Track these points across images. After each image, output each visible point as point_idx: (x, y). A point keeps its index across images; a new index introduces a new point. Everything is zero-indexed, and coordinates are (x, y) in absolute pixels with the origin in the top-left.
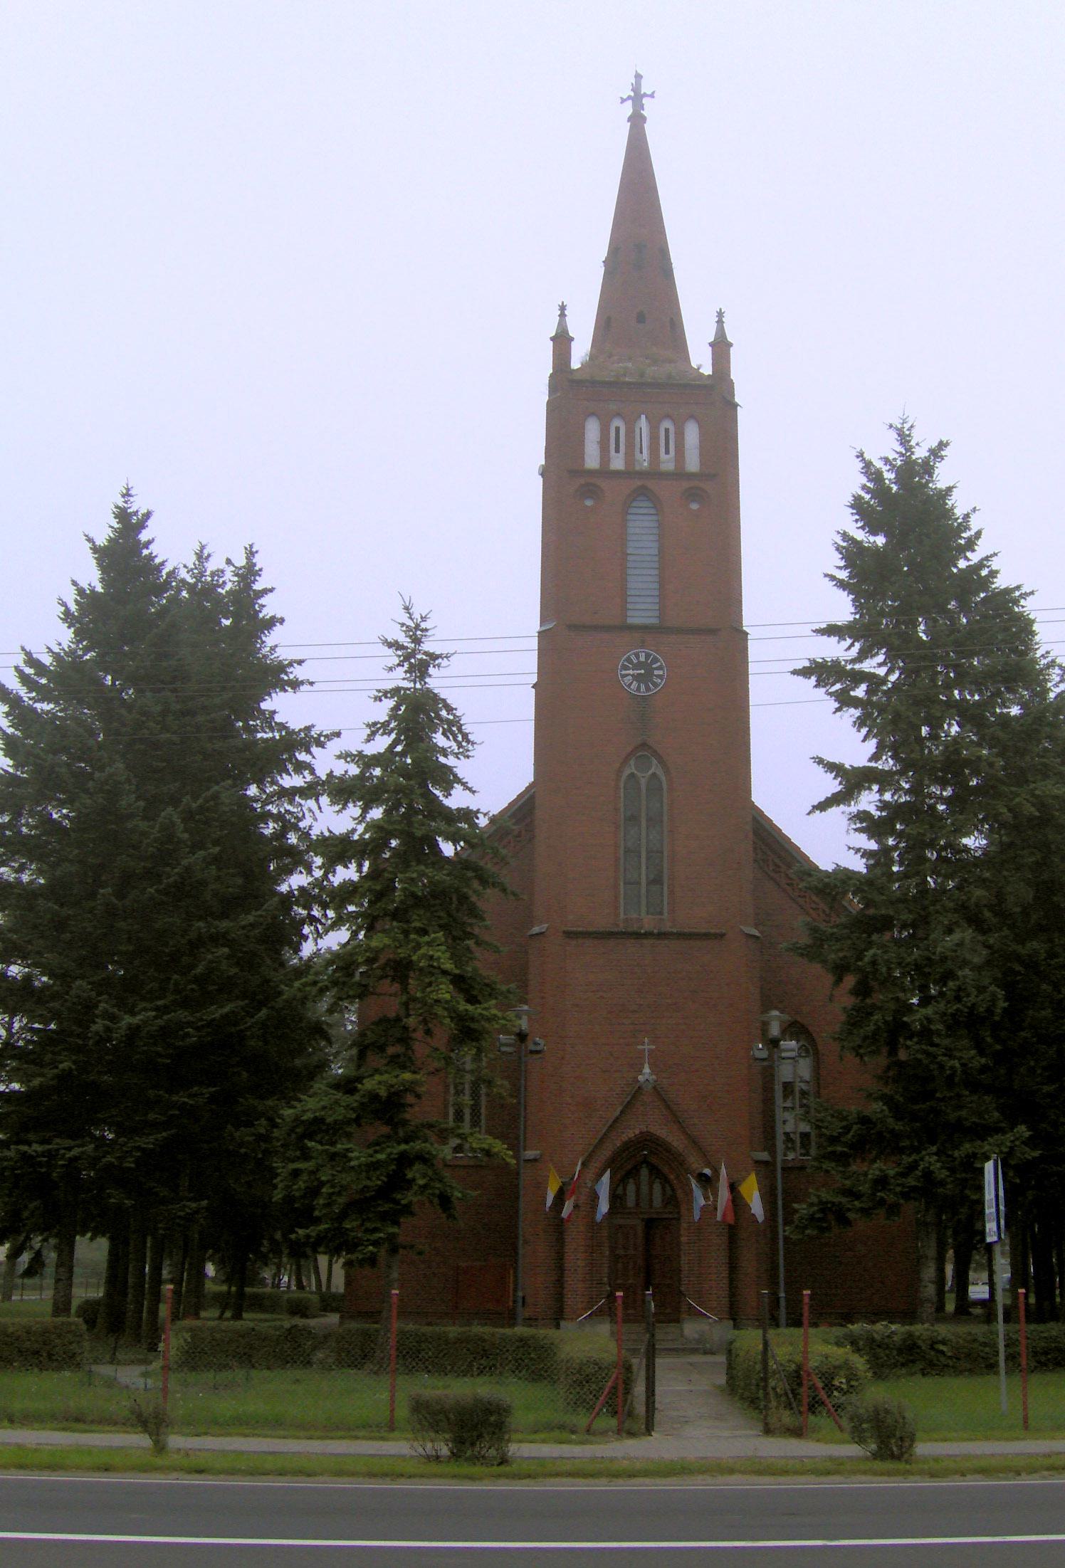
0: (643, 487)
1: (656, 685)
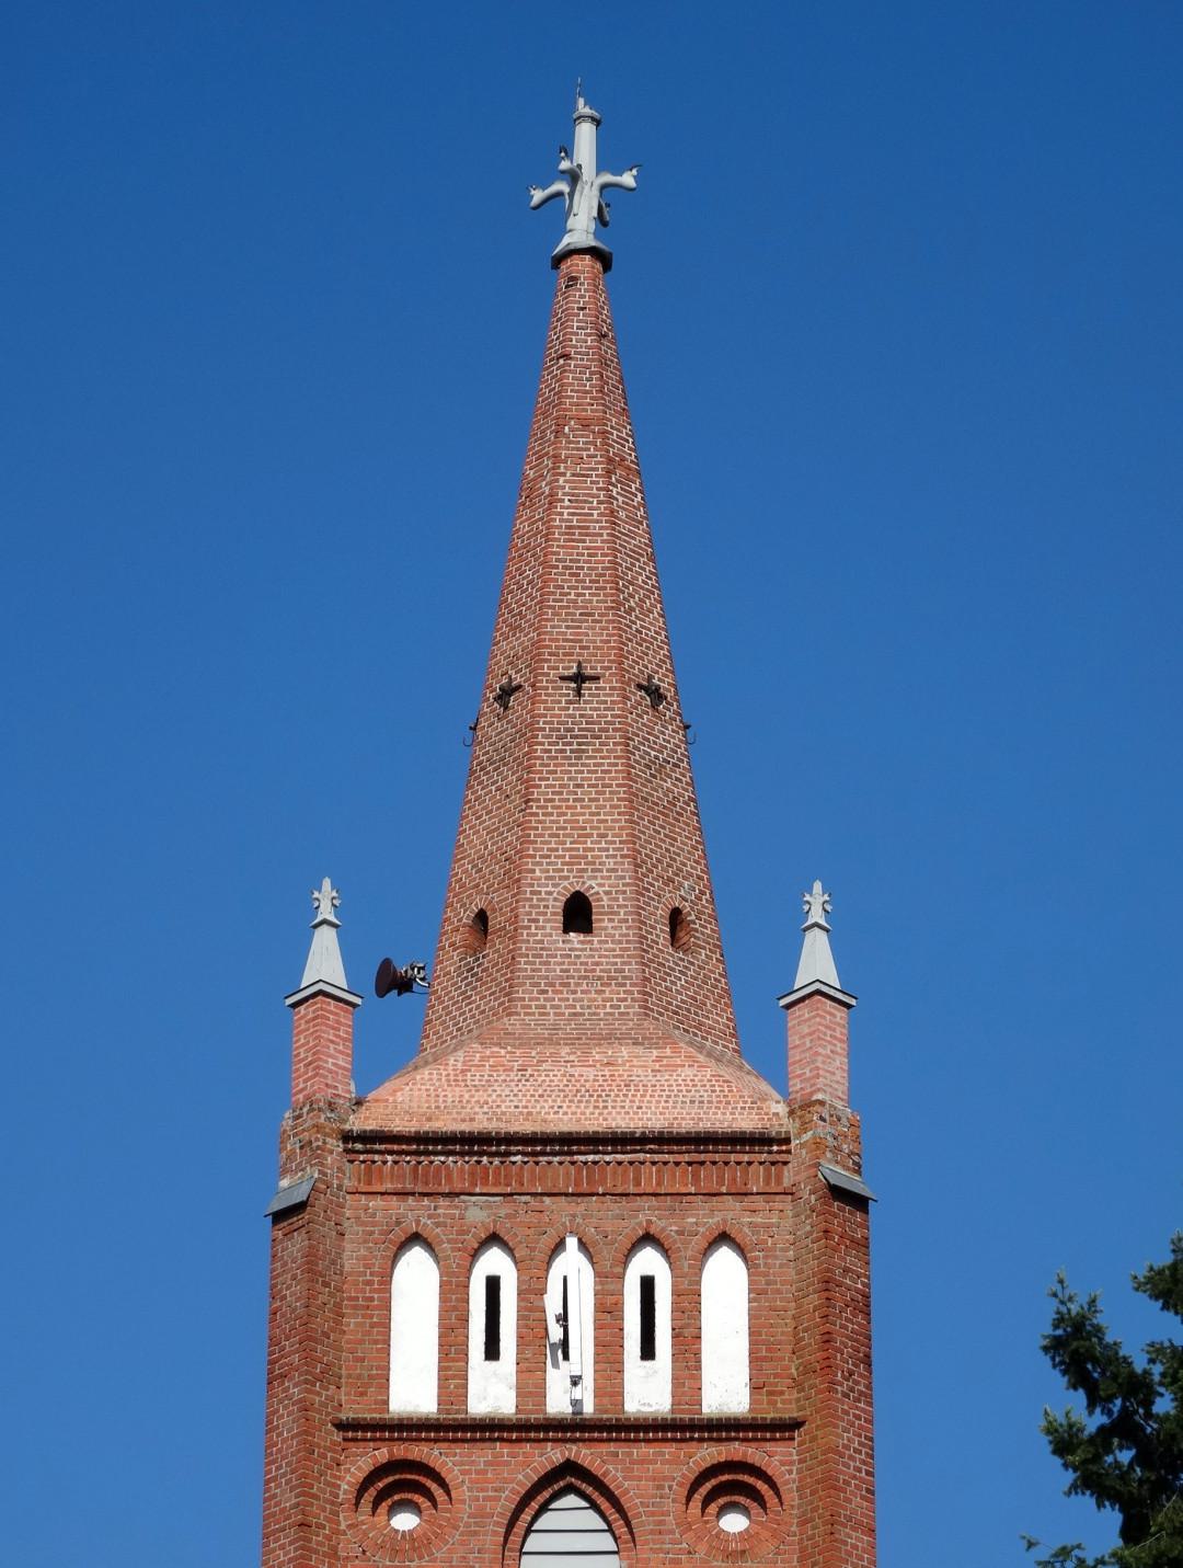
0: (570, 1467)
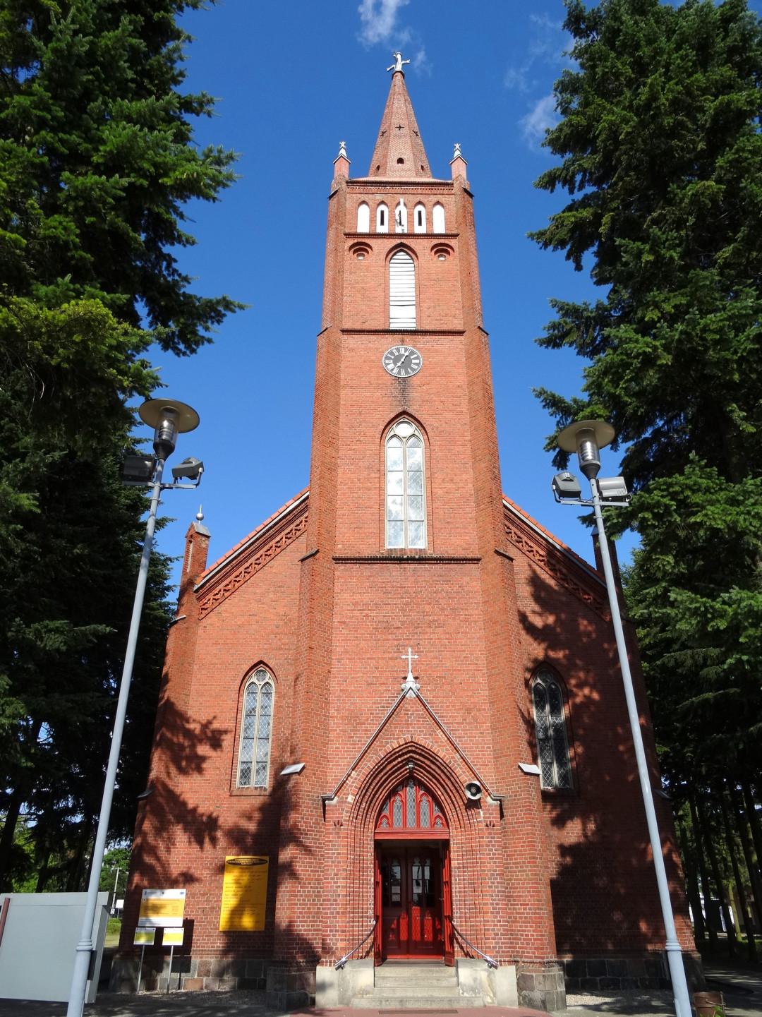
0: (402, 245)
1: (413, 370)
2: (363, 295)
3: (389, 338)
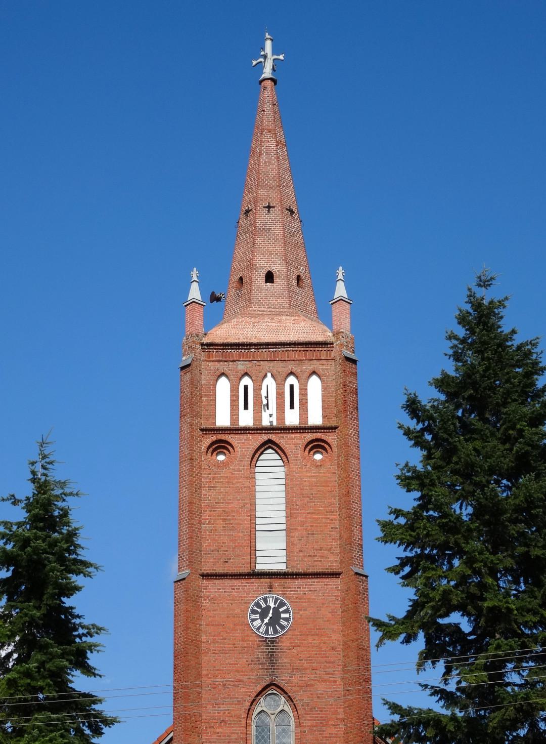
0: (270, 441)
1: (283, 627)
2: (224, 520)
3: (256, 583)
